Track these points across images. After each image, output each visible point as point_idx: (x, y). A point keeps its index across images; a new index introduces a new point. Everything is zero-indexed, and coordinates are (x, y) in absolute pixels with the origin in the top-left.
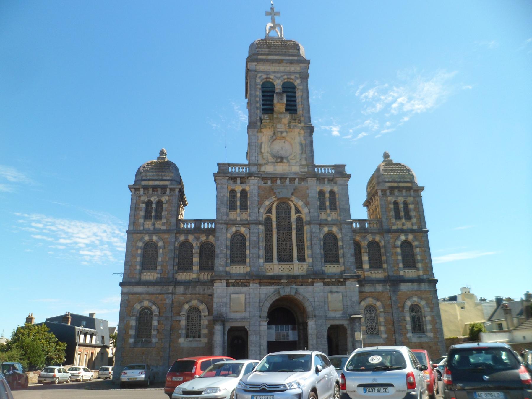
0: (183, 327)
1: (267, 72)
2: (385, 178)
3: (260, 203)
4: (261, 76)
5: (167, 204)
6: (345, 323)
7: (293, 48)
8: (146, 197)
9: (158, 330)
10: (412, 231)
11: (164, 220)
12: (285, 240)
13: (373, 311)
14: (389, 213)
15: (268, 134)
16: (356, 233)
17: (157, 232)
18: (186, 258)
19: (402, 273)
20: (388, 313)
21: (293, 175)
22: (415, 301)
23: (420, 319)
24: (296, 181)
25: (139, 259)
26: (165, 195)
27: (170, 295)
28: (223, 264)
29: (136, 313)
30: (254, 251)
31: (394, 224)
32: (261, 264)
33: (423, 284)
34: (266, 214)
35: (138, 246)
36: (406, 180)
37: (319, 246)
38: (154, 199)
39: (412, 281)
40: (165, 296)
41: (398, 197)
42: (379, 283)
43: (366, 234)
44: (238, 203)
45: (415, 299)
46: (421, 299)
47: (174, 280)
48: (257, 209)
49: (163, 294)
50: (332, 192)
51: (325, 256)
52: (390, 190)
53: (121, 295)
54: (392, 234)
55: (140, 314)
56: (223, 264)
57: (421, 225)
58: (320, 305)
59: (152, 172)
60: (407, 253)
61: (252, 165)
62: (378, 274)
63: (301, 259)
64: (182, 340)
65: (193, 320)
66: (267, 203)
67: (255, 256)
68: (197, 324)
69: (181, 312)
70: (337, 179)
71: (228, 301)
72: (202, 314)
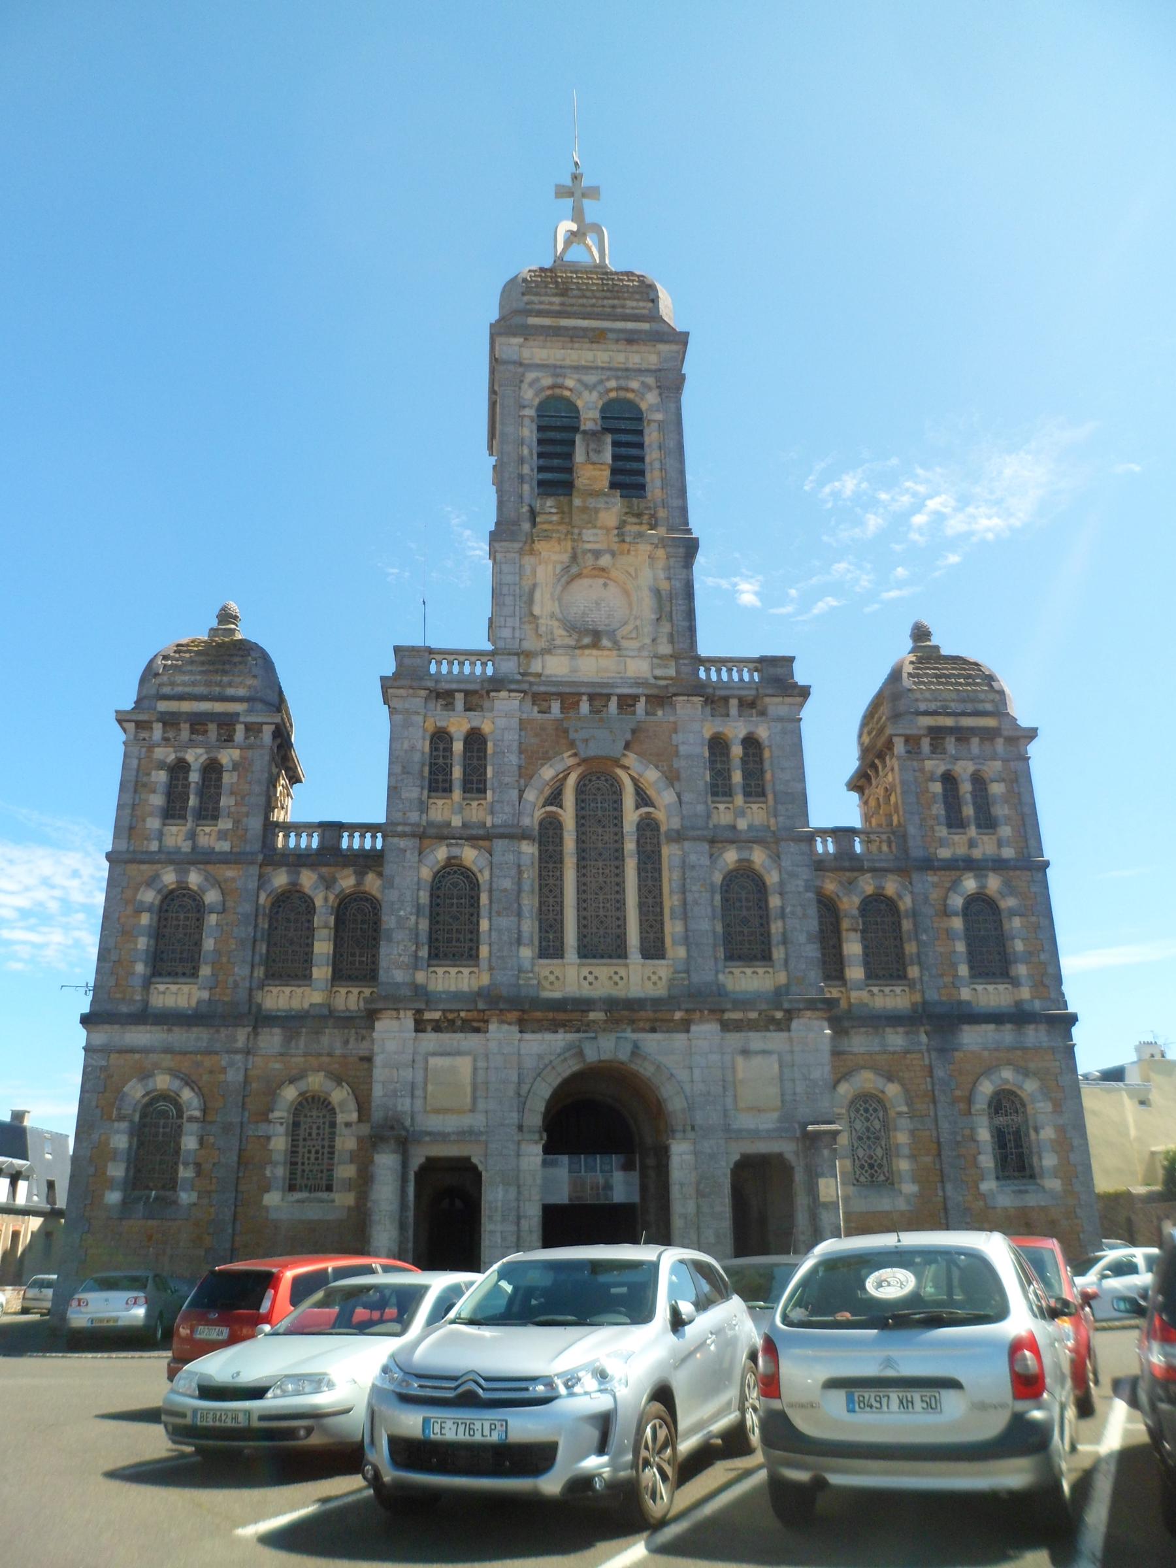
0: (279, 1157)
1: (555, 367)
2: (917, 700)
3: (526, 774)
4: (537, 380)
5: (235, 774)
6: (787, 1148)
7: (637, 297)
8: (171, 749)
9: (198, 1165)
10: (999, 865)
11: (225, 824)
12: (601, 888)
13: (875, 1110)
14: (929, 808)
15: (555, 557)
16: (827, 871)
17: (202, 858)
18: (292, 943)
19: (965, 994)
20: (922, 1117)
21: (631, 687)
22: (1006, 1081)
23: (1022, 1135)
24: (641, 706)
25: (142, 943)
26: (231, 744)
27: (239, 1057)
28: (406, 960)
29: (130, 1112)
30: (504, 922)
31: (942, 843)
32: (527, 965)
33: (1032, 1027)
34: (544, 806)
35: (141, 902)
36: (980, 707)
37: (709, 910)
38: (195, 757)
39: (996, 1018)
40: (224, 1060)
41: (956, 759)
42: (894, 1026)
43: (856, 874)
44: (457, 772)
45: (1007, 1074)
46: (1026, 1073)
47: (254, 1009)
48: (515, 794)
49: (217, 1053)
50: (751, 743)
52: (932, 739)
53: (83, 1053)
54: (938, 873)
55: (143, 1116)
56: (406, 960)
57: (1027, 847)
58: (709, 1093)
59: (191, 673)
60: (982, 933)
61: (503, 654)
62: (894, 999)
63: (653, 949)
64: (273, 1199)
65: (310, 1134)
66: (548, 773)
67: (505, 938)
68: (323, 1147)
69: (272, 1111)
70: (767, 700)
71: (420, 1078)
72: (341, 1118)
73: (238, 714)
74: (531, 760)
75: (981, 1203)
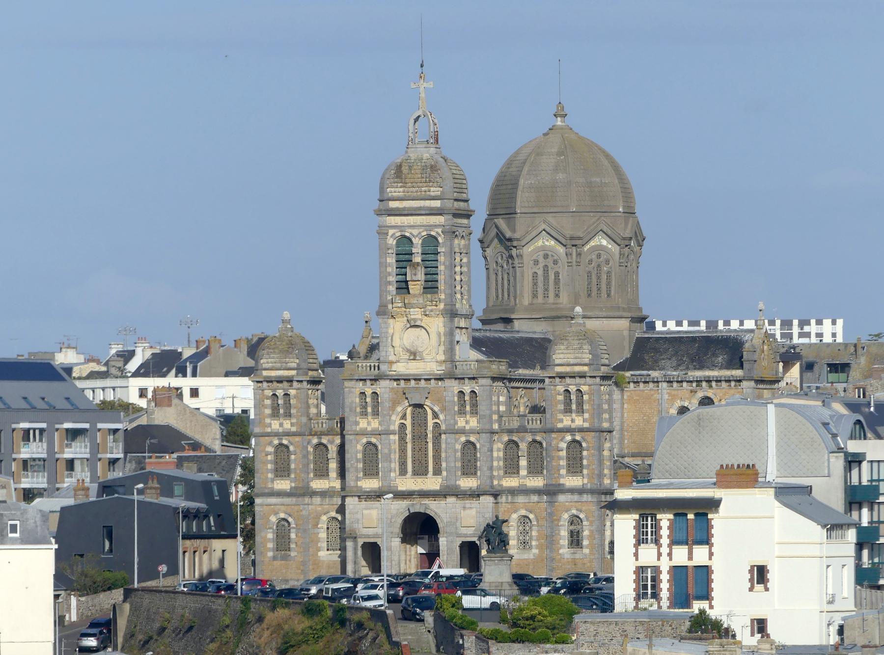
3: (393, 408)
9: (296, 543)
13: (527, 523)
17: (288, 434)
27: (306, 506)
30: (386, 465)
62: (538, 482)
64: (321, 554)
66: (399, 409)
73: (293, 376)
75: (559, 557)
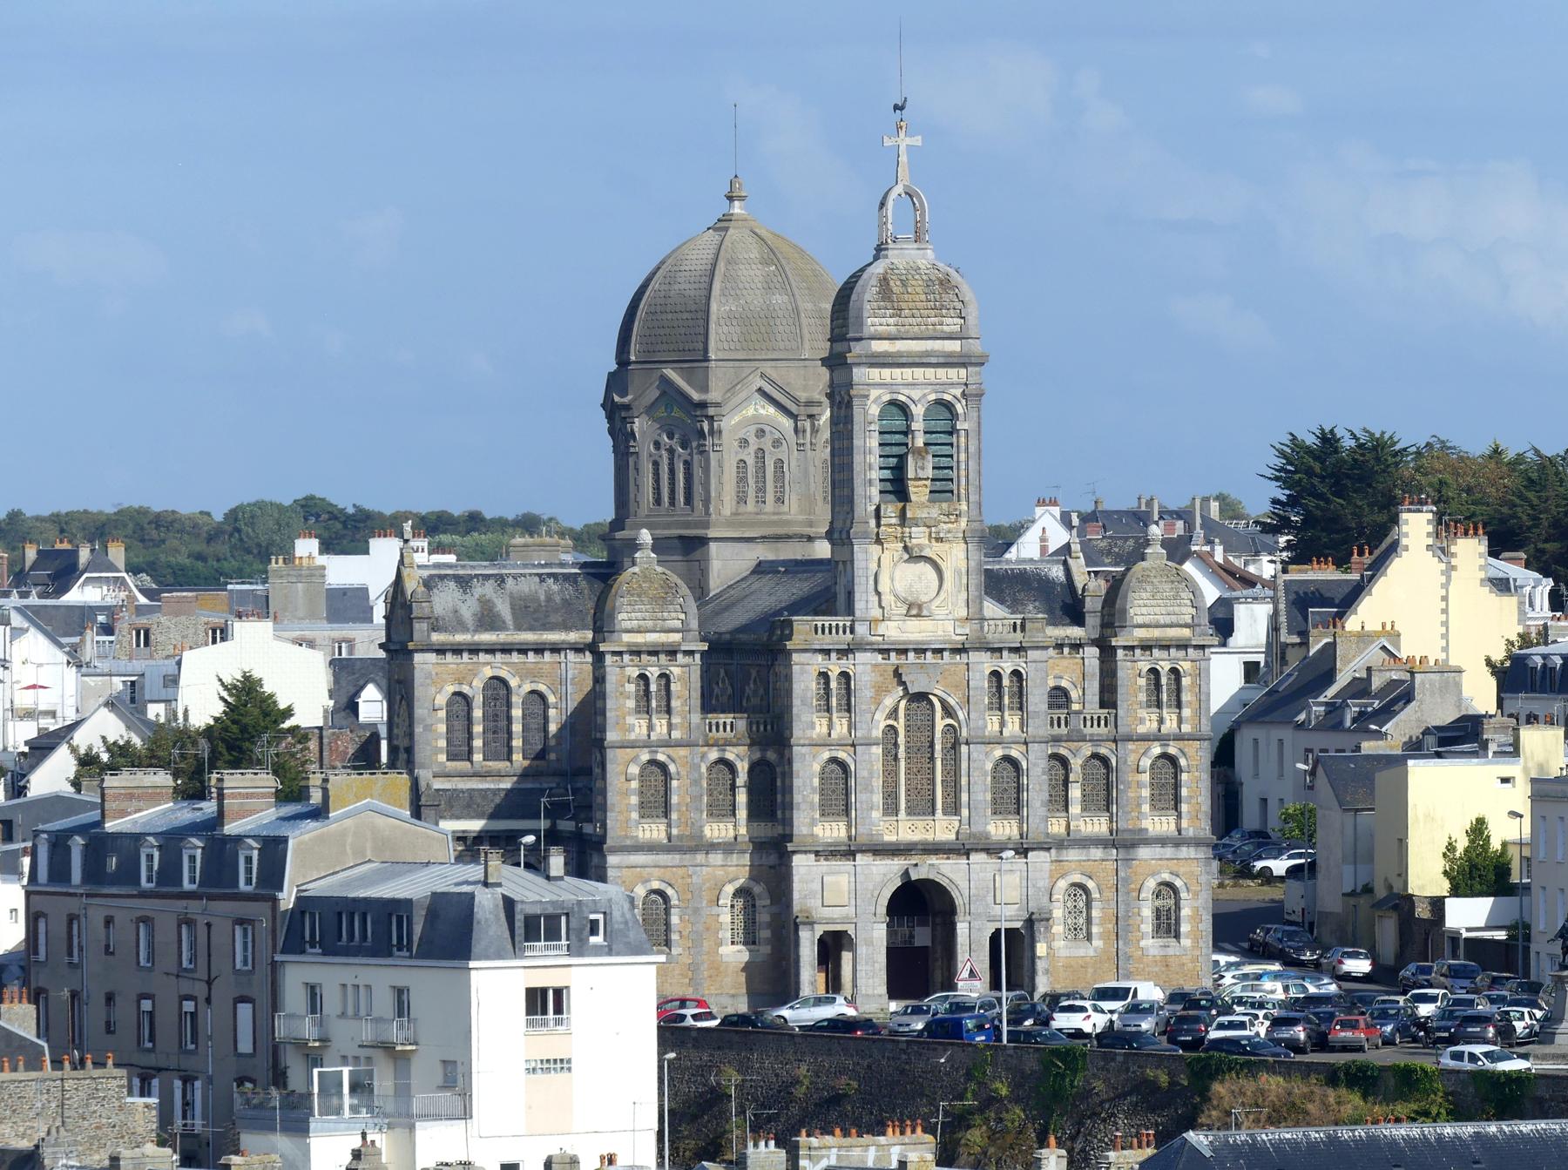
4: (879, 397)
9: (680, 932)
26: (674, 663)
31: (1142, 721)
38: (653, 672)
39: (1162, 841)
43: (1081, 744)
48: (870, 715)
51: (994, 801)
63: (953, 808)
67: (865, 806)
74: (881, 691)
